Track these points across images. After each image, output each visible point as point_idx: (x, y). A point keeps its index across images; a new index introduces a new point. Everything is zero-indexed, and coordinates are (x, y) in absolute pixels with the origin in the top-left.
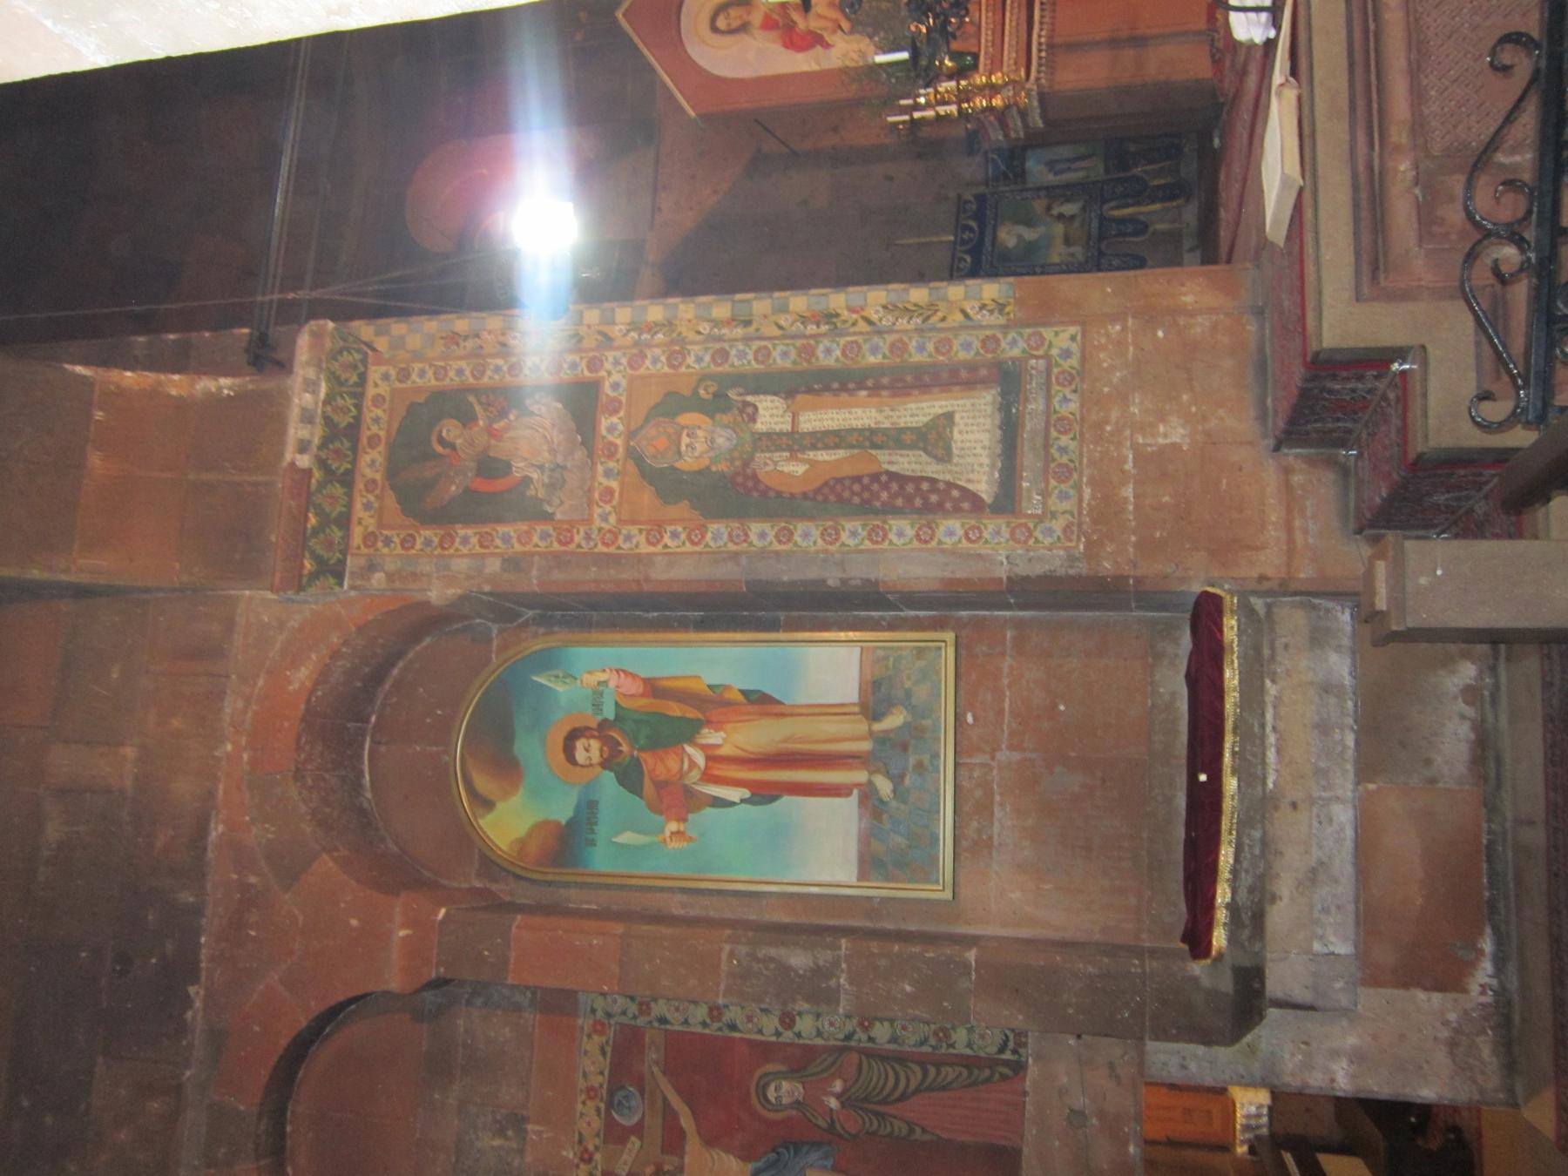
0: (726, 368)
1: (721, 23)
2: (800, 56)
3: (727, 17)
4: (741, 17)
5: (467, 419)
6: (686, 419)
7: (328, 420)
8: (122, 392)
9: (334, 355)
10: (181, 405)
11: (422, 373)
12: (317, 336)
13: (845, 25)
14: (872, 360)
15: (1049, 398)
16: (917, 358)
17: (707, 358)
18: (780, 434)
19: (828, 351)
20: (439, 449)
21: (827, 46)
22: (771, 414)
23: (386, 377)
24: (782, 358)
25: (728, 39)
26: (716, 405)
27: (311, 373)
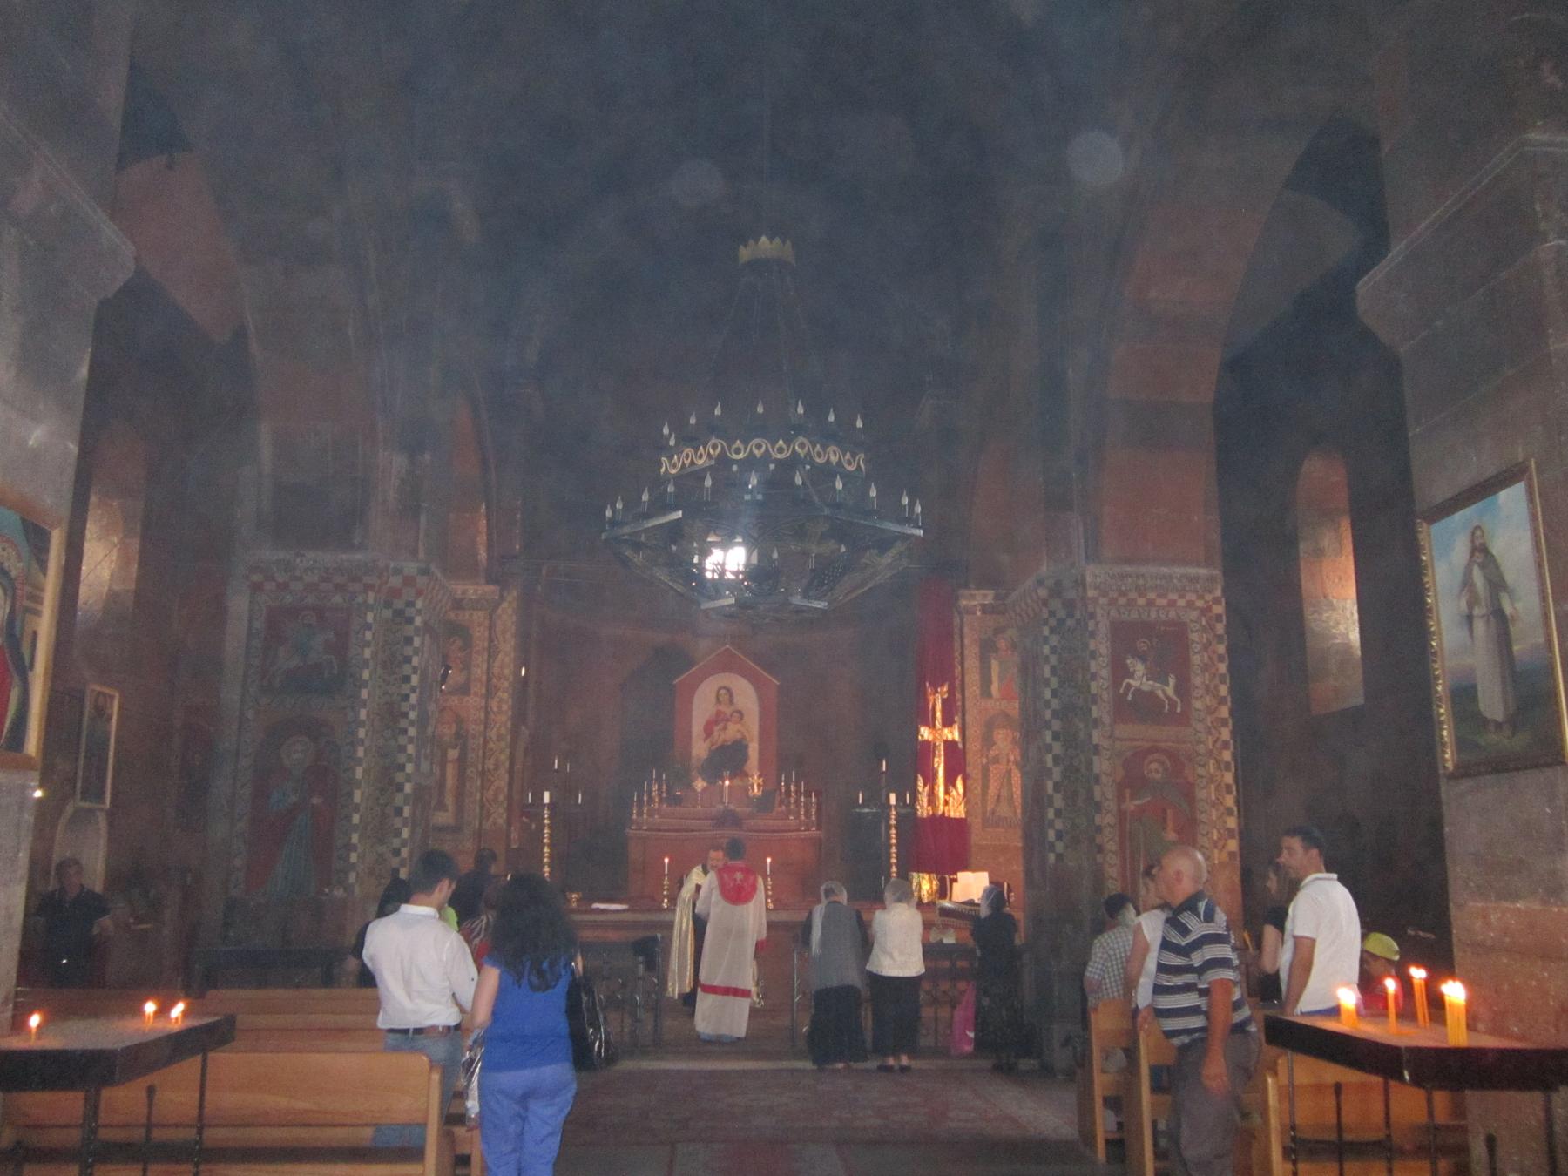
1: (723, 692)
2: (702, 728)
3: (725, 694)
6: (454, 726)
7: (462, 600)
11: (479, 632)
13: (714, 747)
14: (468, 785)
15: (449, 841)
16: (467, 801)
17: (473, 732)
18: (446, 757)
19: (472, 772)
20: (452, 640)
21: (705, 739)
22: (453, 754)
23: (479, 618)
24: (471, 756)
26: (458, 735)
27: (480, 592)
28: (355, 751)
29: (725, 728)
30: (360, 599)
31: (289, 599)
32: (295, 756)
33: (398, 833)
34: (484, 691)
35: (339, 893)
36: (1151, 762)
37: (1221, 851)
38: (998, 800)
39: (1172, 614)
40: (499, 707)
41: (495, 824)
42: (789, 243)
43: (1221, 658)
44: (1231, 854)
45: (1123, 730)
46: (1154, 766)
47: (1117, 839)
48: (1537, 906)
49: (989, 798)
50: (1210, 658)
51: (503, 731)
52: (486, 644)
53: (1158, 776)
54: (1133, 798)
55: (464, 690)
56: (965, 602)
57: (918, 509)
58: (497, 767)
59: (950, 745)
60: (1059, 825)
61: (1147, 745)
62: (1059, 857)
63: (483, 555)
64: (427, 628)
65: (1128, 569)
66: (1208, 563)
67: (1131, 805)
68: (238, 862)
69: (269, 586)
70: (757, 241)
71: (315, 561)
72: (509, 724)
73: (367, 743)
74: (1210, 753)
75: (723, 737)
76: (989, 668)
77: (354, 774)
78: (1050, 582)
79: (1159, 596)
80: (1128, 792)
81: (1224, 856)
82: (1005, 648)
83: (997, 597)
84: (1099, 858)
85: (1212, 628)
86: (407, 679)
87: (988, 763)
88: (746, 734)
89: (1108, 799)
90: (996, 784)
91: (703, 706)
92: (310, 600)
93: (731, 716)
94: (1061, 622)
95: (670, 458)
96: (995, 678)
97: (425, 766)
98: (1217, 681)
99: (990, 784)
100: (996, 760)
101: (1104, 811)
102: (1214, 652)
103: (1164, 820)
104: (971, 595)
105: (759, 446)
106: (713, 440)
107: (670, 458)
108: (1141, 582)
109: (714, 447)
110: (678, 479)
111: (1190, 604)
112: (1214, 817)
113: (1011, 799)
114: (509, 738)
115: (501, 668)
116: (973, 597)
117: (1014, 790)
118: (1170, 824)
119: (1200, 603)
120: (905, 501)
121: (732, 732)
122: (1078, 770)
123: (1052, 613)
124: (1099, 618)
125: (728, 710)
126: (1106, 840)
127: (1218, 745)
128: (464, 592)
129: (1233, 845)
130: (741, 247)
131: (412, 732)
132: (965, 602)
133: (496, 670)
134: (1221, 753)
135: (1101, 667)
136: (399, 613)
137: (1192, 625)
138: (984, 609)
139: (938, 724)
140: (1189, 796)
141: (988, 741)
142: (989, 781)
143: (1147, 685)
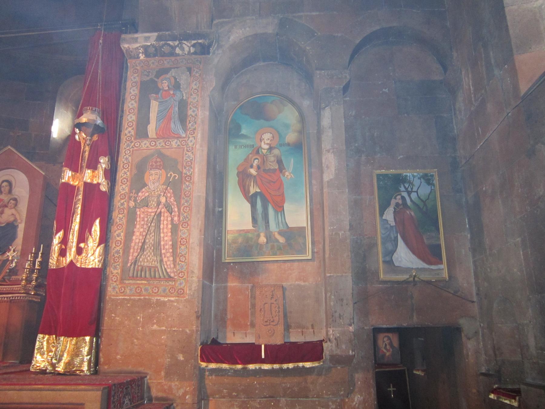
1: (5, 184)
3: (6, 186)
4: (5, 191)
38: (142, 249)
49: (133, 244)
56: (126, 46)
82: (167, 88)
83: (159, 39)
87: (135, 207)
88: (18, 217)
90: (142, 230)
96: (153, 115)
99: (135, 230)
104: (133, 38)
113: (157, 246)
116: (136, 40)
117: (162, 235)
132: (126, 46)
138: (146, 48)
142: (135, 226)
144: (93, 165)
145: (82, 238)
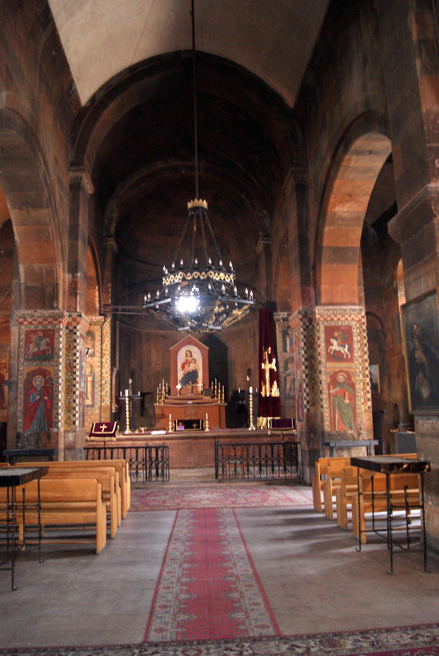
0: (96, 373)
1: (188, 352)
5: (91, 340)
6: (90, 369)
8: (95, 293)
9: (100, 322)
10: (94, 300)
12: (102, 319)
13: (185, 373)
14: (96, 390)
16: (96, 396)
21: (182, 370)
22: (90, 379)
25: (185, 354)
26: (91, 372)
27: (97, 319)
28: (59, 381)
29: (189, 365)
30: (57, 327)
31: (32, 327)
32: (37, 383)
33: (75, 409)
34: (100, 355)
35: (55, 430)
36: (340, 376)
37: (365, 406)
38: (290, 390)
39: (347, 323)
40: (106, 361)
41: (106, 404)
42: (205, 201)
43: (365, 338)
44: (369, 407)
45: (329, 365)
46: (341, 377)
47: (328, 403)
48: (435, 421)
50: (361, 338)
51: (108, 370)
52: (100, 338)
53: (342, 381)
54: (333, 388)
55: (93, 355)
57: (251, 294)
58: (106, 383)
59: (271, 370)
60: (308, 398)
61: (338, 370)
62: (308, 410)
63: (97, 305)
64: (81, 335)
65: (331, 307)
66: (360, 304)
67: (332, 391)
68: (20, 420)
69: (26, 323)
70: (193, 200)
71: (41, 313)
72: (110, 367)
73: (62, 377)
74: (361, 372)
75: (188, 369)
76: (286, 341)
77: (58, 388)
78: (303, 313)
79: (342, 316)
80: (332, 387)
81: (366, 408)
84: (322, 410)
85: (361, 327)
86: (75, 354)
88: (197, 368)
89: (324, 389)
91: (181, 357)
92: (40, 327)
93: (192, 361)
94: (307, 327)
95: (166, 279)
97: (82, 385)
98: (363, 346)
100: (289, 375)
101: (323, 394)
102: (362, 335)
103: (345, 396)
105: (196, 275)
106: (180, 273)
107: (166, 279)
108: (335, 312)
109: (181, 275)
110: (169, 287)
111: (353, 319)
112: (362, 394)
114: (110, 372)
115: (106, 346)
118: (347, 397)
119: (356, 319)
120: (247, 292)
121: (192, 367)
122: (314, 379)
123: (304, 324)
124: (320, 325)
125: (190, 359)
126: (324, 404)
127: (364, 368)
128: (91, 319)
129: (370, 404)
130: (188, 203)
131: (78, 373)
133: (104, 347)
134: (365, 371)
135: (322, 342)
136: (71, 331)
137: (353, 327)
139: (267, 362)
140: (353, 386)
141: (286, 368)
143: (338, 349)
144: (270, 362)
145: (271, 387)
